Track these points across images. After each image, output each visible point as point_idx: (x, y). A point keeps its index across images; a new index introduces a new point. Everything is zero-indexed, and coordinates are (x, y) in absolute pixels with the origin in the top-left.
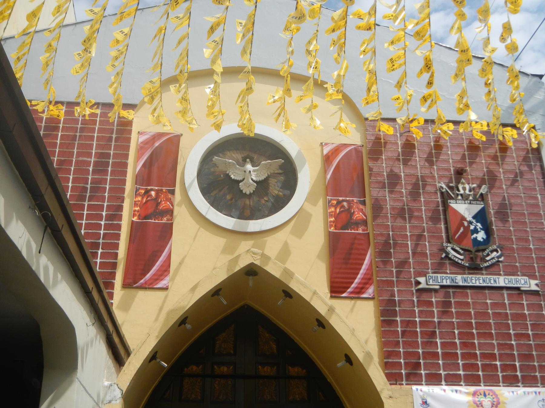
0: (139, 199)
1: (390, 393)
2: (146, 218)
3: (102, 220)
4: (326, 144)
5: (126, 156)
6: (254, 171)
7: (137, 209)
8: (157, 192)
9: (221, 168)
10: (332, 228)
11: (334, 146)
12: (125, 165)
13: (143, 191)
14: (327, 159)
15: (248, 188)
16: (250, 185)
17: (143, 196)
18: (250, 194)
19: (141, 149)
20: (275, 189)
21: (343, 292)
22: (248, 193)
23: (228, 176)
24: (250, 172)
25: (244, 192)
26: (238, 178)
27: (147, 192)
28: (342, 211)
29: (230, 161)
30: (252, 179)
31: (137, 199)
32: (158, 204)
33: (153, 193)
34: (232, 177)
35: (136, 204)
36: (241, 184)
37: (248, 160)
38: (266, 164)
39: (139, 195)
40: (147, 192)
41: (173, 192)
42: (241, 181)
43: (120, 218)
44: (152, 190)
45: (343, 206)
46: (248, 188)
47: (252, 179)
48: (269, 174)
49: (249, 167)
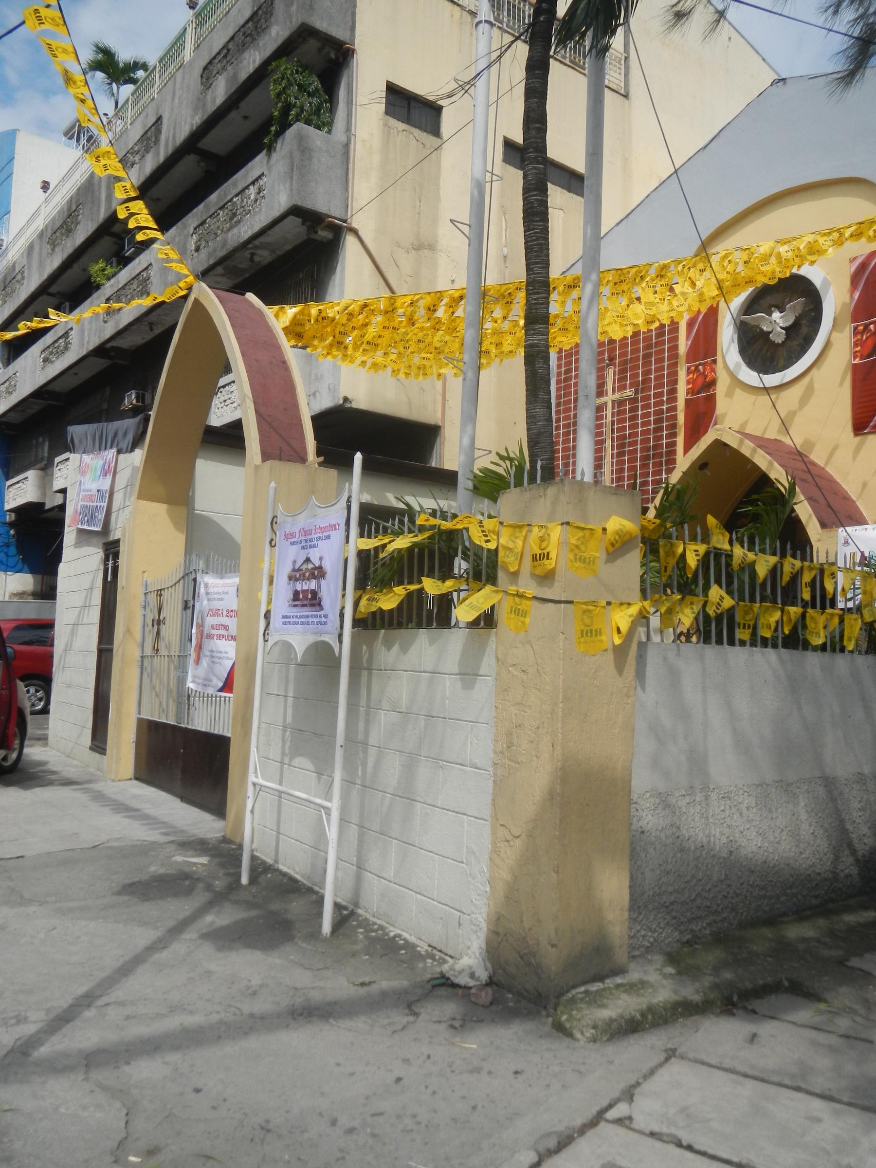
0: (691, 376)
1: (819, 537)
2: (699, 392)
3: (663, 405)
4: (855, 259)
5: (676, 339)
6: (782, 317)
7: (690, 386)
8: (704, 365)
9: (753, 323)
10: (858, 359)
11: (863, 257)
12: (676, 347)
13: (693, 368)
14: (855, 278)
15: (778, 336)
16: (780, 333)
17: (693, 373)
18: (783, 342)
19: (690, 324)
20: (804, 330)
21: (865, 428)
22: (780, 342)
23: (762, 330)
24: (775, 321)
25: (776, 342)
26: (770, 330)
27: (697, 367)
28: (870, 336)
29: (759, 314)
30: (781, 328)
31: (689, 377)
32: (706, 376)
33: (701, 367)
34: (765, 328)
35: (688, 382)
36: (771, 335)
37: (773, 309)
38: (790, 308)
39: (691, 372)
40: (697, 367)
41: (715, 362)
42: (770, 333)
43: (675, 399)
44: (700, 364)
45: (870, 330)
46: (778, 336)
47: (781, 328)
48: (797, 315)
49: (776, 315)
